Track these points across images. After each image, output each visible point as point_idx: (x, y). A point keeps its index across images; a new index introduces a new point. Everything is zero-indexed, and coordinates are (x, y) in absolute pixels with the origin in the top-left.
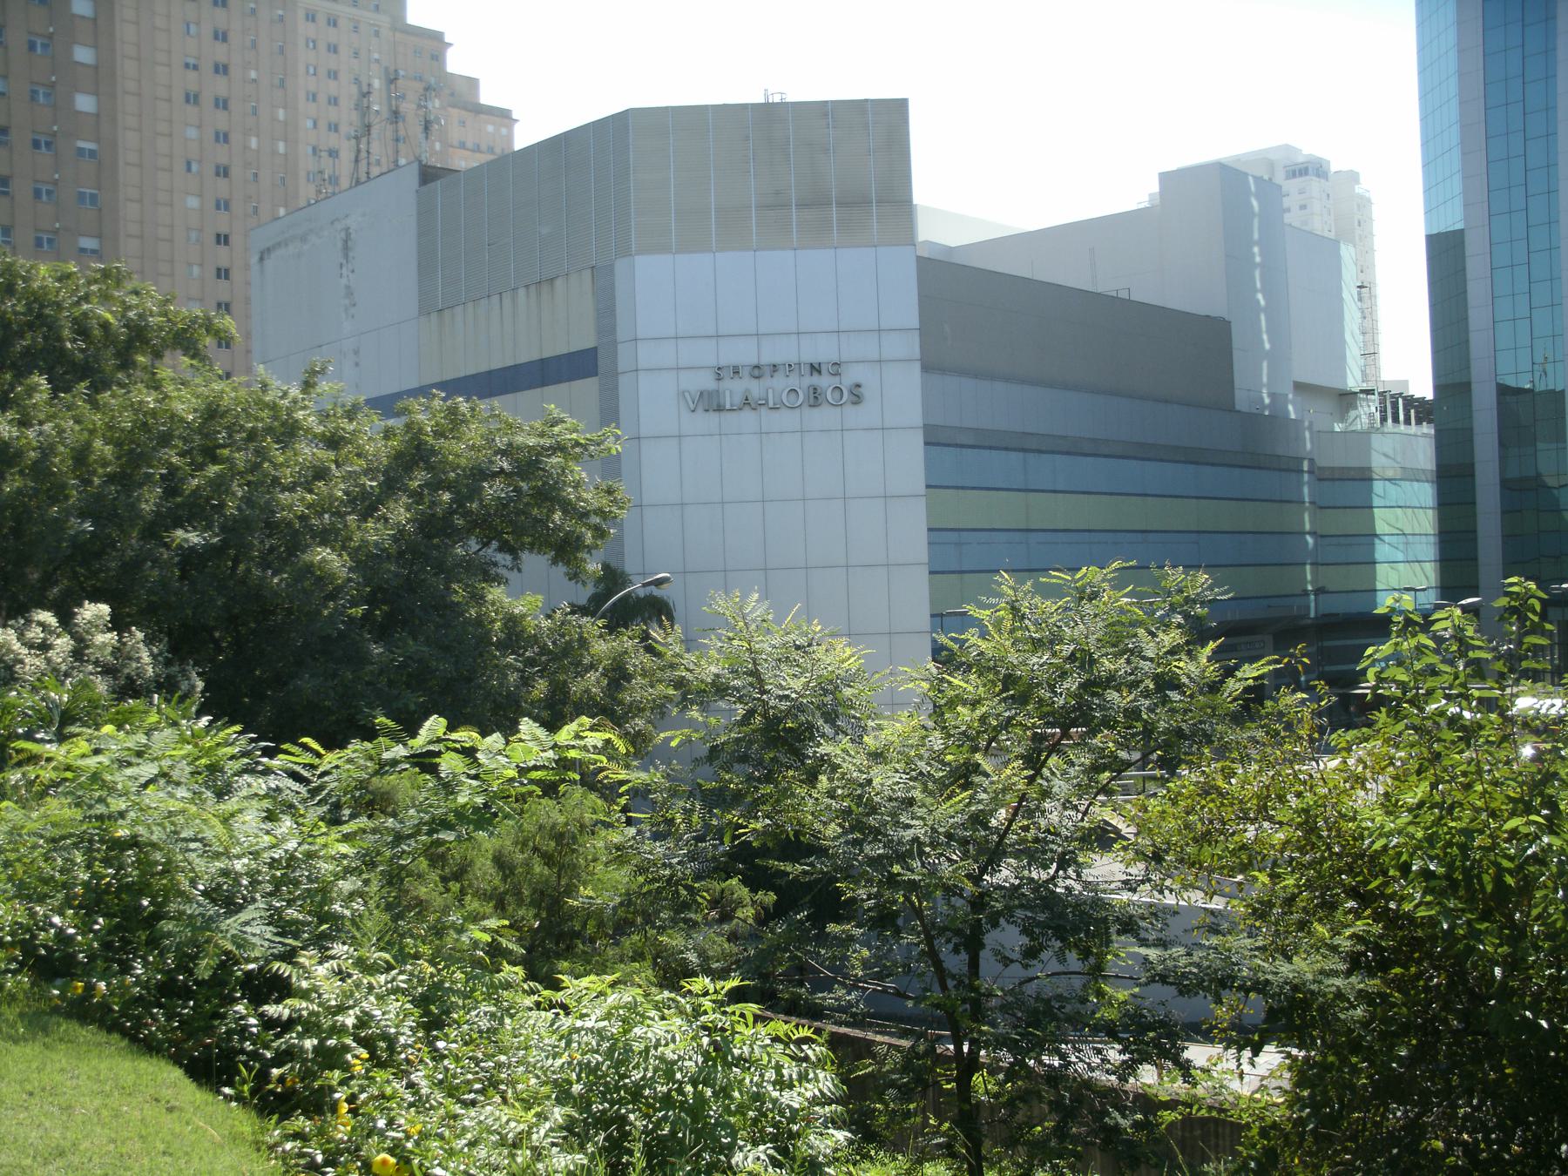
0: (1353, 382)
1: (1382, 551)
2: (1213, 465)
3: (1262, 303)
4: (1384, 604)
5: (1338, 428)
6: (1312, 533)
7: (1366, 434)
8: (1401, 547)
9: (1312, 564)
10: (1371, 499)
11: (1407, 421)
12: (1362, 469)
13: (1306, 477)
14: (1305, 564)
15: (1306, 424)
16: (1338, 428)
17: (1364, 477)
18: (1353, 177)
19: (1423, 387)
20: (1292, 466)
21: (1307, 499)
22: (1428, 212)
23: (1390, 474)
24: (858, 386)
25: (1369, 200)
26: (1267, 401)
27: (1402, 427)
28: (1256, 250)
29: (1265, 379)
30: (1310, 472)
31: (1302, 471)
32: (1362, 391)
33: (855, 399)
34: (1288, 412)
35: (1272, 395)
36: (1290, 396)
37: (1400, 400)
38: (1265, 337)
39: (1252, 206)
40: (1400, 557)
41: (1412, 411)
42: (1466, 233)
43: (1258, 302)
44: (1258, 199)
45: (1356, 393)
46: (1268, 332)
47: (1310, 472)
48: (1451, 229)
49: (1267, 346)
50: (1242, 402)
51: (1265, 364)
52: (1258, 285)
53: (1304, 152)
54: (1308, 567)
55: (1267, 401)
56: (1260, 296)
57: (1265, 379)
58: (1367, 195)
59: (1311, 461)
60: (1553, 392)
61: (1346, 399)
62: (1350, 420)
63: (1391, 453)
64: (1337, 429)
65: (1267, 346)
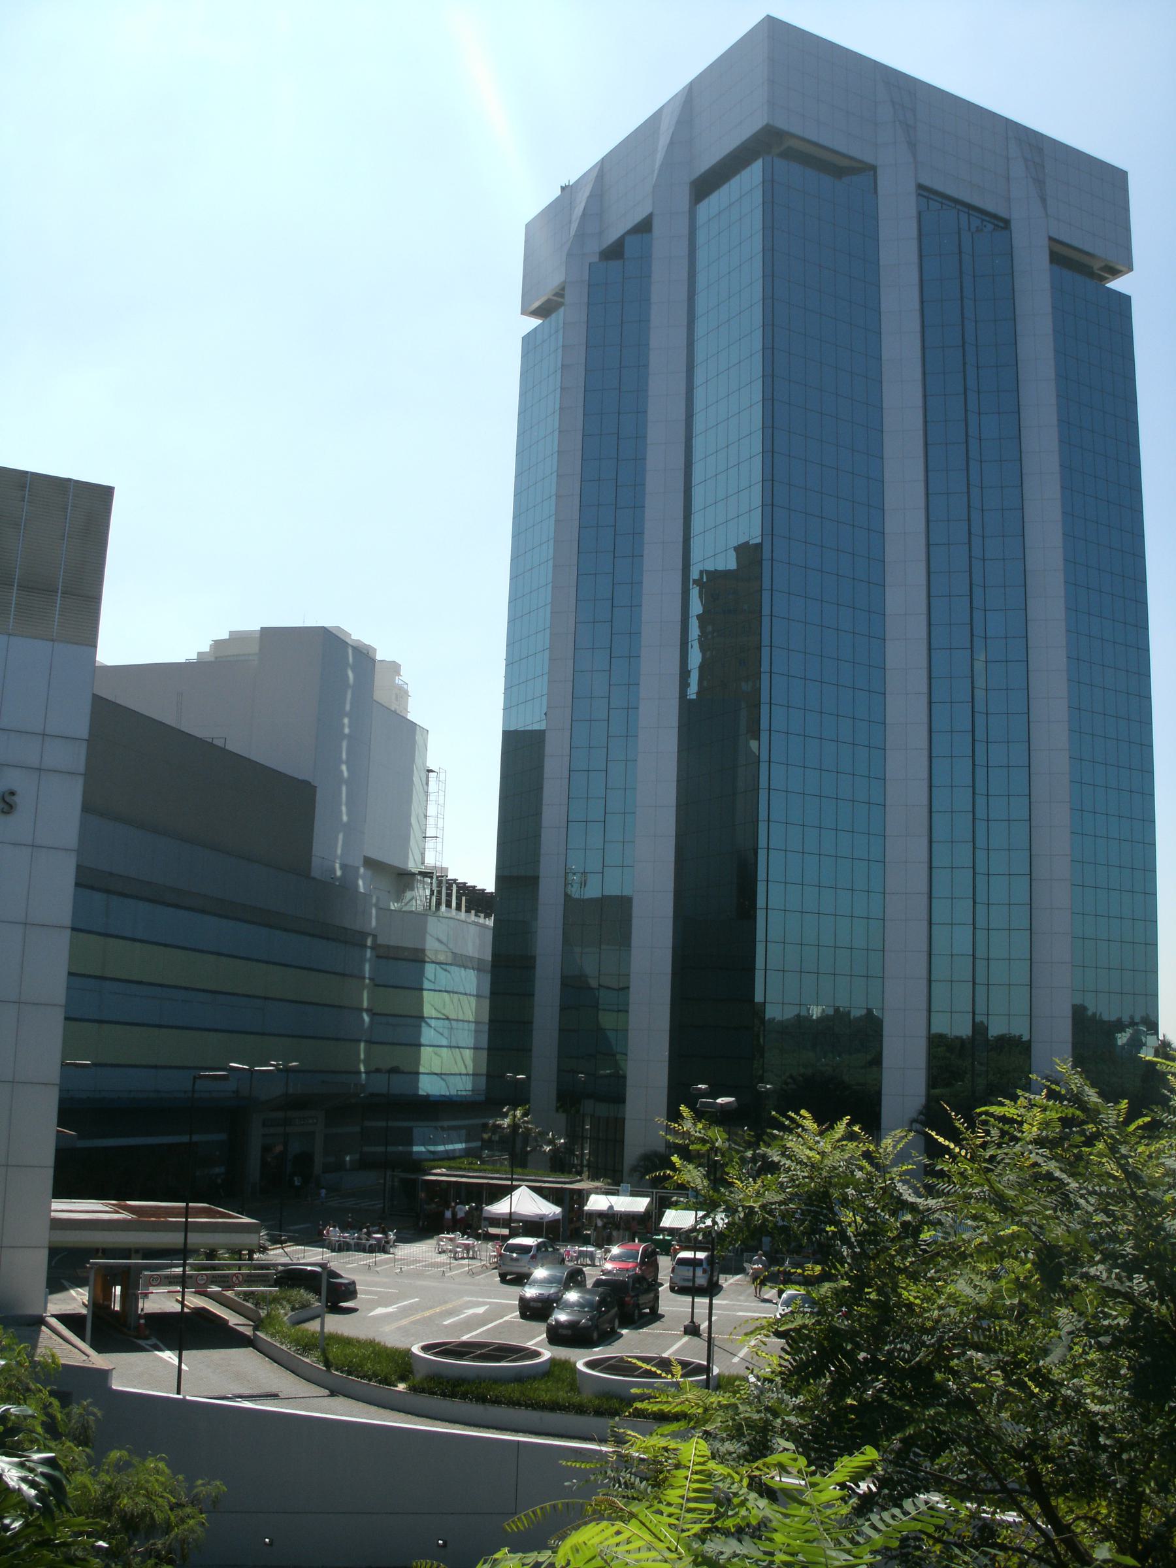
0: (412, 866)
1: (428, 1035)
2: (285, 930)
3: (346, 774)
4: (428, 1086)
5: (394, 906)
6: (368, 1011)
7: (420, 919)
8: (446, 1033)
9: (366, 1041)
10: (422, 983)
11: (459, 908)
12: (75, 933)
13: (369, 953)
14: (359, 1041)
15: (374, 900)
16: (394, 906)
17: (417, 958)
18: (395, 668)
19: (486, 881)
20: (354, 939)
21: (367, 976)
22: (506, 709)
23: (441, 958)
24: (13, 793)
25: (406, 692)
26: (339, 873)
27: (454, 912)
28: (346, 721)
29: (339, 851)
30: (372, 948)
31: (365, 946)
32: (421, 873)
33: (6, 808)
34: (357, 886)
35: (344, 867)
36: (362, 870)
37: (454, 886)
38: (344, 809)
39: (348, 677)
40: (444, 1042)
41: (464, 899)
42: (548, 735)
43: (342, 772)
44: (353, 672)
45: (414, 874)
46: (347, 805)
47: (372, 948)
48: (529, 728)
49: (345, 818)
50: (315, 873)
51: (341, 836)
52: (344, 756)
53: (353, 638)
54: (362, 1045)
55: (339, 873)
56: (344, 768)
57: (339, 851)
58: (405, 686)
59: (375, 937)
60: (621, 897)
61: (404, 879)
62: (405, 901)
63: (444, 939)
64: (392, 908)
65: (345, 818)
